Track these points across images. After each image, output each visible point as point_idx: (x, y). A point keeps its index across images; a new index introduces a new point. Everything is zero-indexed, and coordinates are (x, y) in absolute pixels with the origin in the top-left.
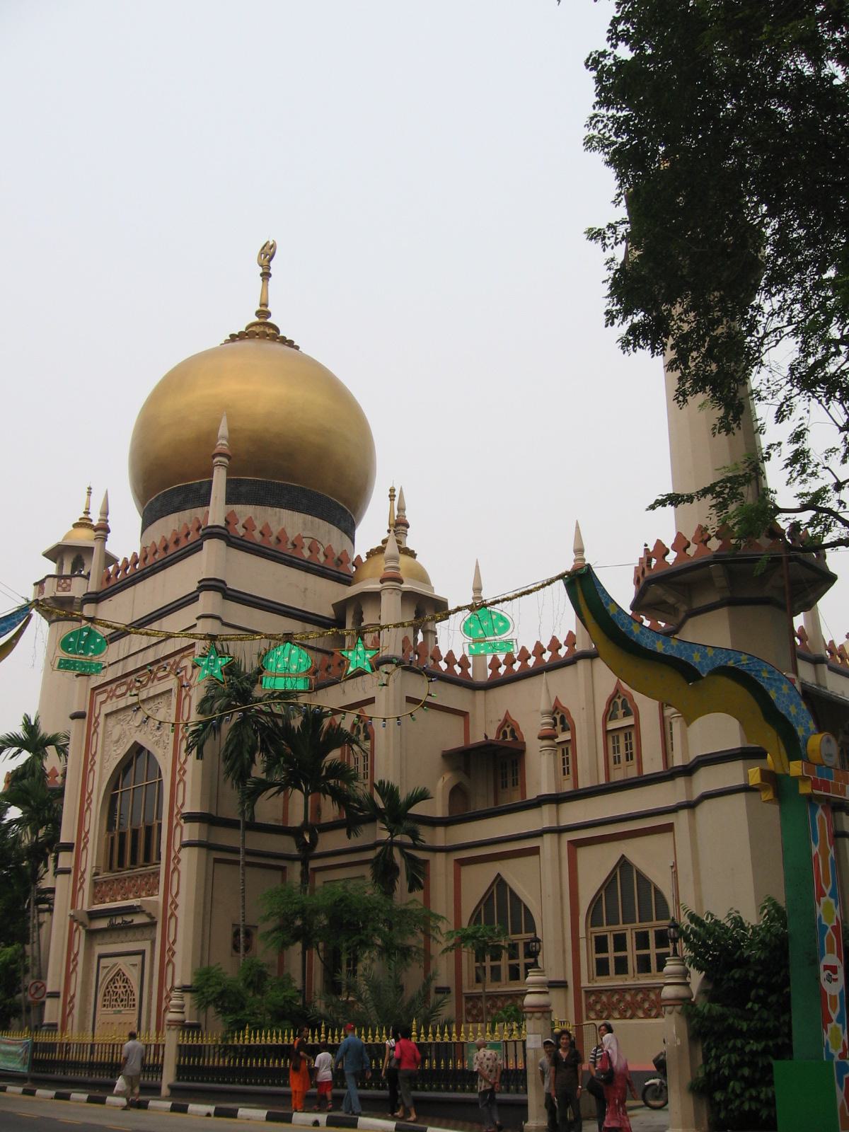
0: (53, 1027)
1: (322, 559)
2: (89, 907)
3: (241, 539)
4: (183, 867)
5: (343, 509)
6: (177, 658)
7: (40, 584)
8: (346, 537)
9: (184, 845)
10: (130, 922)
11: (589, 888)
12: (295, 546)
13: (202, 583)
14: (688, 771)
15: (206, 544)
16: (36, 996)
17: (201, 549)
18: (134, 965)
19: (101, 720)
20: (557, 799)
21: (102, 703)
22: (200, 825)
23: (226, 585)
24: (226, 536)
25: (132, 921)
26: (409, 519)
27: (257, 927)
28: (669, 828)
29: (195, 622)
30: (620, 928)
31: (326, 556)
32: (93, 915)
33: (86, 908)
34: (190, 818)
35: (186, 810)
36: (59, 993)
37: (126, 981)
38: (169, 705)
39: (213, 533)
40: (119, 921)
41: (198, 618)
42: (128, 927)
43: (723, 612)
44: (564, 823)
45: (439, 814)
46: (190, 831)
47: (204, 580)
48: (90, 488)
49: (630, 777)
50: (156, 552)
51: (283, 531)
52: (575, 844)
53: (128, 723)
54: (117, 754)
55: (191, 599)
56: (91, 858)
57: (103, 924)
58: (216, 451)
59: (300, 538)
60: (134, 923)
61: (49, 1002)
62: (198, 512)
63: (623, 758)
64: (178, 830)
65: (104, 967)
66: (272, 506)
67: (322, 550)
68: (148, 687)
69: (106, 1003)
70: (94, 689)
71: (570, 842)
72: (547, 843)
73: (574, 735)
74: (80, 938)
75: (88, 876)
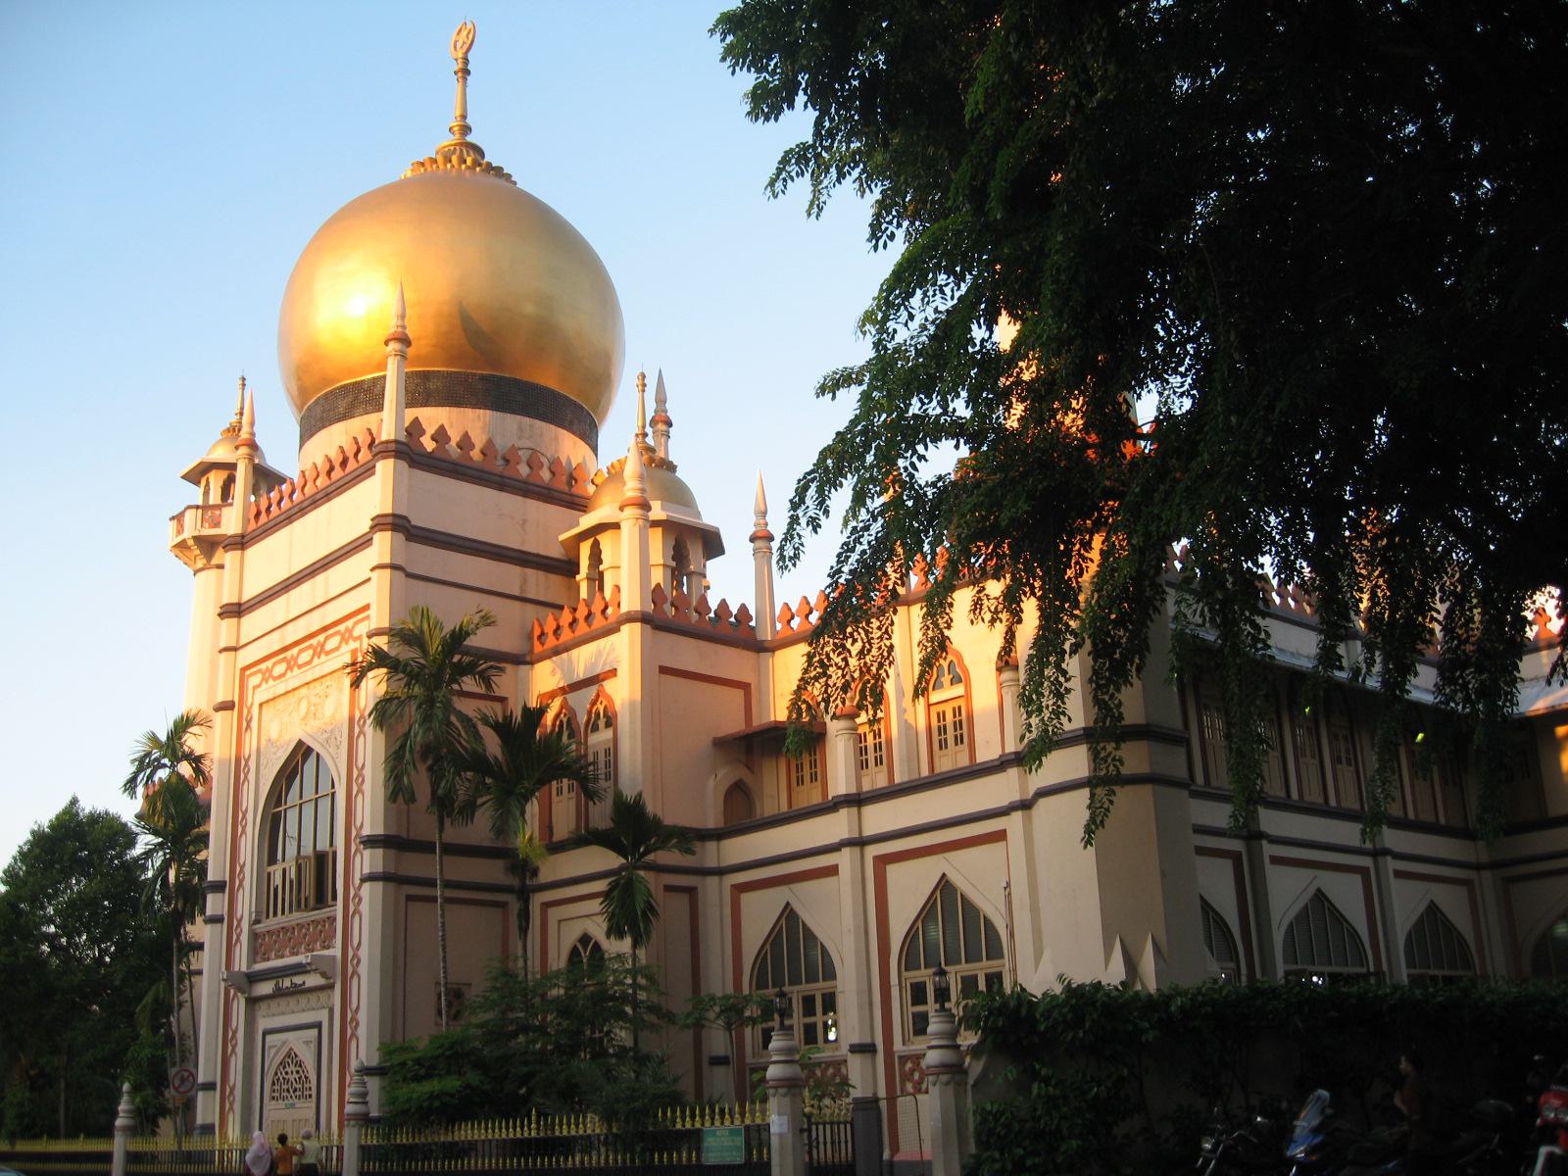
0: (208, 1129)
1: (546, 475)
2: (248, 967)
5: (575, 403)
6: (349, 623)
7: (178, 518)
9: (363, 880)
10: (301, 985)
11: (902, 918)
12: (507, 461)
13: (376, 522)
16: (182, 1089)
17: (374, 473)
18: (307, 1043)
19: (255, 710)
20: (857, 801)
22: (384, 856)
23: (409, 522)
24: (407, 454)
25: (304, 983)
27: (470, 985)
28: (1000, 836)
29: (370, 574)
32: (253, 978)
33: (244, 969)
34: (371, 842)
35: (366, 831)
38: (341, 690)
40: (287, 983)
41: (373, 569)
42: (298, 991)
44: (868, 831)
47: (378, 516)
48: (244, 379)
49: (960, 765)
52: (882, 861)
53: (290, 715)
55: (362, 544)
56: (246, 902)
59: (514, 449)
60: (307, 985)
62: (369, 420)
63: (951, 741)
64: (358, 858)
65: (270, 1048)
68: (314, 664)
69: (276, 1094)
70: (244, 669)
71: (876, 858)
72: (845, 859)
74: (239, 1006)
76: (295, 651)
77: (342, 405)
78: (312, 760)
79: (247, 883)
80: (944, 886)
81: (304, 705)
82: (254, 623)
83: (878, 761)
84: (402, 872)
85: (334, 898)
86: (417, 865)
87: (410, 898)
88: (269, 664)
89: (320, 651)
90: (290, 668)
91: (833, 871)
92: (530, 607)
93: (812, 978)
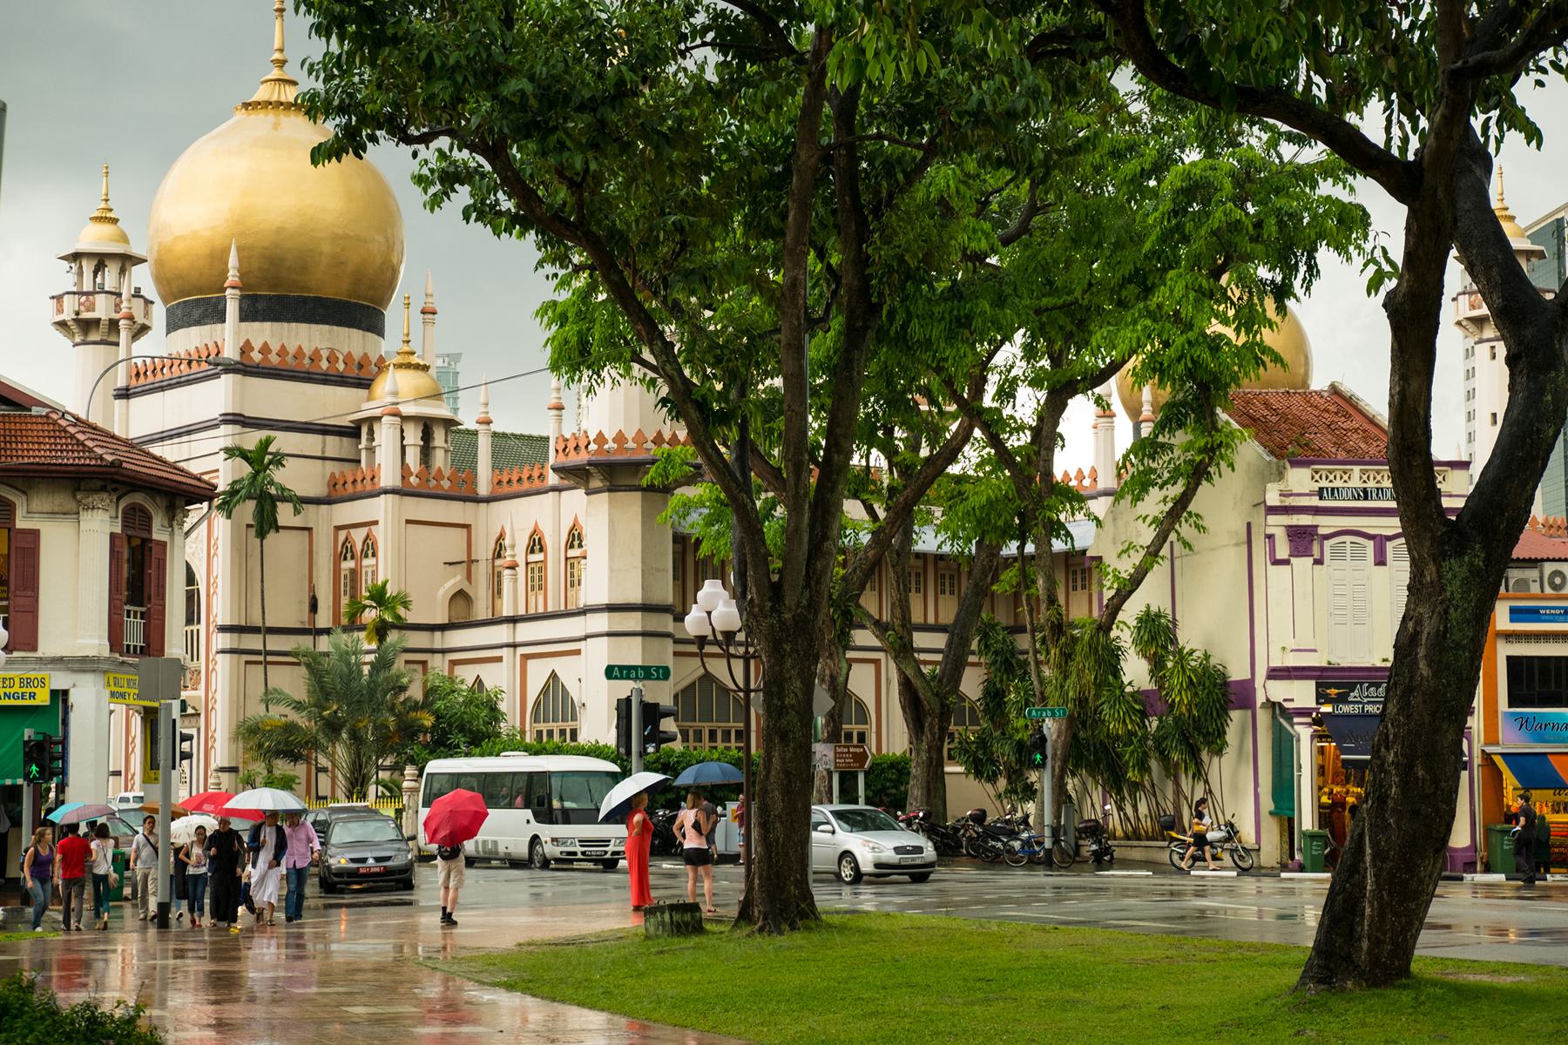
1: (341, 367)
3: (257, 366)
4: (218, 668)
14: (584, 612)
20: (513, 620)
30: (551, 725)
34: (223, 629)
35: (220, 622)
46: (223, 641)
51: (300, 348)
59: (317, 351)
66: (289, 321)
71: (522, 655)
72: (504, 652)
73: (546, 556)
77: (196, 313)
80: (554, 676)
83: (540, 589)
84: (242, 647)
86: (254, 642)
87: (247, 663)
91: (499, 659)
92: (328, 463)
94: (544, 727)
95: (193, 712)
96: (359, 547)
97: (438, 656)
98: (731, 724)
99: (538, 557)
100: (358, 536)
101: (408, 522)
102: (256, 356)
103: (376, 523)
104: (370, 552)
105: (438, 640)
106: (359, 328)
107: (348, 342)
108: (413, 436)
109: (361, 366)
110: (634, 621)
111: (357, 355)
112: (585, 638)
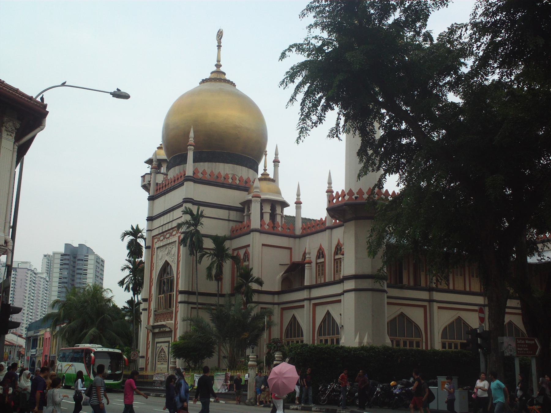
0: (142, 369)
1: (238, 182)
2: (153, 324)
3: (200, 179)
8: (251, 171)
9: (181, 302)
12: (225, 178)
13: (184, 200)
14: (341, 281)
15: (185, 183)
17: (184, 185)
18: (166, 346)
19: (156, 249)
20: (310, 288)
21: (156, 242)
26: (280, 159)
29: (182, 215)
30: (327, 337)
31: (240, 181)
32: (154, 327)
33: (152, 325)
34: (181, 292)
35: (180, 288)
36: (144, 356)
37: (164, 352)
39: (188, 179)
43: (352, 223)
45: (277, 290)
46: (180, 298)
50: (172, 182)
51: (219, 173)
52: (315, 305)
54: (161, 264)
57: (157, 330)
58: (188, 144)
59: (227, 175)
61: (141, 360)
67: (238, 178)
70: (153, 237)
72: (306, 303)
73: (325, 260)
74: (151, 334)
75: (152, 312)
76: (165, 234)
78: (169, 266)
79: (153, 300)
80: (328, 313)
81: (167, 249)
82: (157, 223)
85: (173, 307)
87: (192, 308)
88: (159, 236)
89: (171, 235)
90: (164, 238)
92: (231, 222)
93: (298, 336)
94: (323, 338)
95: (169, 330)
96: (242, 257)
97: (276, 306)
98: (413, 338)
99: (322, 260)
100: (242, 252)
101: (263, 245)
102: (200, 175)
103: (249, 246)
104: (247, 259)
105: (276, 299)
106: (246, 166)
107: (243, 172)
108: (267, 209)
109: (246, 182)
110: (367, 284)
111: (245, 177)
112: (342, 294)
